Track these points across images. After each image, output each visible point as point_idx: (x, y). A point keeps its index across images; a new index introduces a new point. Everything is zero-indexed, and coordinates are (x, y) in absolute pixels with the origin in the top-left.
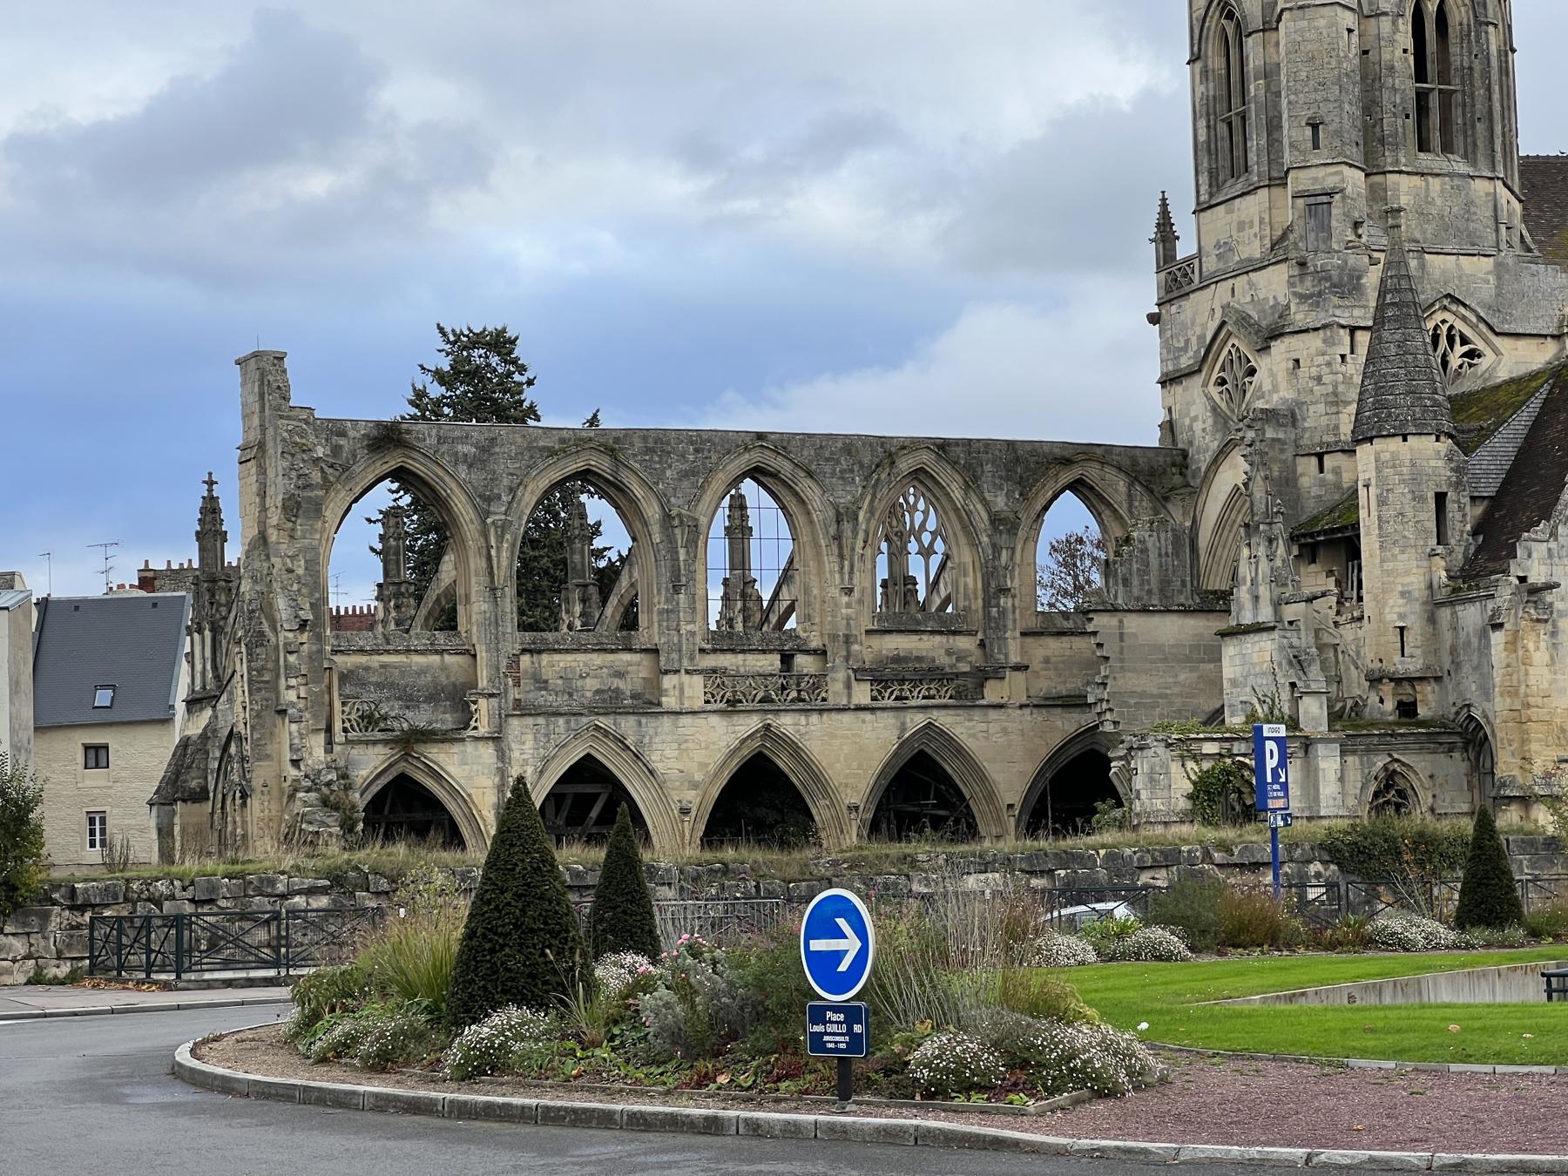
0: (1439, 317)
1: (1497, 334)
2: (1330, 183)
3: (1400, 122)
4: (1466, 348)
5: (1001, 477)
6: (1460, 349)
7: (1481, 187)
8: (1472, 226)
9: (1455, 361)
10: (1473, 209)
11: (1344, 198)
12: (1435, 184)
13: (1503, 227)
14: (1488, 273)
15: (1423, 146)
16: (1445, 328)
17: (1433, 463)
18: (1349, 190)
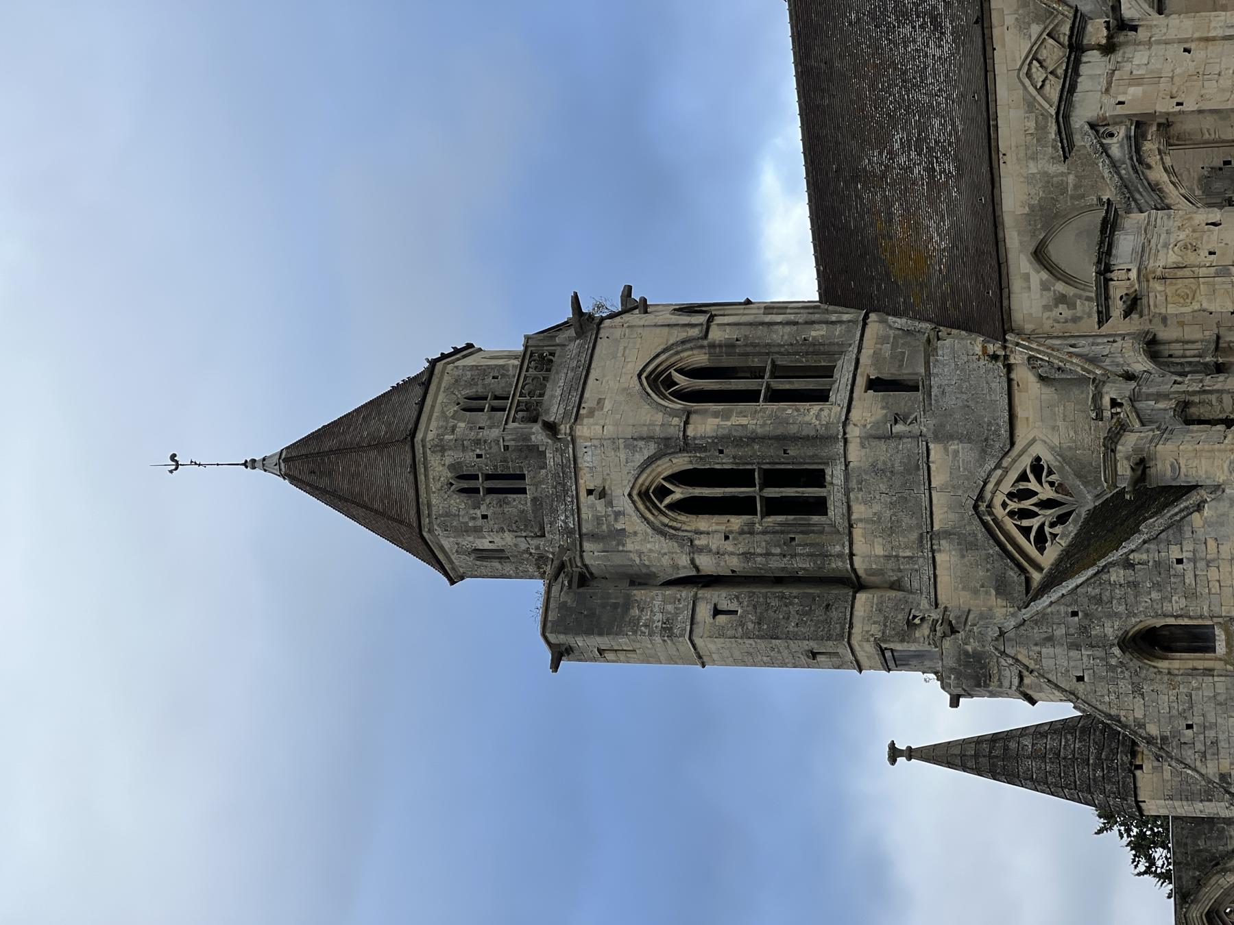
0: (1000, 512)
1: (1012, 444)
2: (870, 648)
3: (799, 550)
4: (1031, 477)
5: (1211, 830)
6: (1033, 485)
7: (856, 454)
8: (898, 468)
9: (1046, 493)
10: (880, 465)
11: (885, 641)
12: (859, 511)
13: (899, 428)
14: (946, 450)
15: (819, 506)
16: (1013, 505)
17: (1167, 775)
18: (875, 630)
